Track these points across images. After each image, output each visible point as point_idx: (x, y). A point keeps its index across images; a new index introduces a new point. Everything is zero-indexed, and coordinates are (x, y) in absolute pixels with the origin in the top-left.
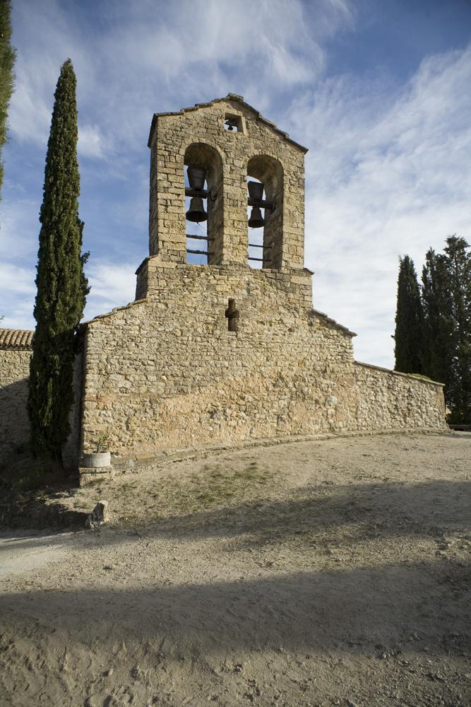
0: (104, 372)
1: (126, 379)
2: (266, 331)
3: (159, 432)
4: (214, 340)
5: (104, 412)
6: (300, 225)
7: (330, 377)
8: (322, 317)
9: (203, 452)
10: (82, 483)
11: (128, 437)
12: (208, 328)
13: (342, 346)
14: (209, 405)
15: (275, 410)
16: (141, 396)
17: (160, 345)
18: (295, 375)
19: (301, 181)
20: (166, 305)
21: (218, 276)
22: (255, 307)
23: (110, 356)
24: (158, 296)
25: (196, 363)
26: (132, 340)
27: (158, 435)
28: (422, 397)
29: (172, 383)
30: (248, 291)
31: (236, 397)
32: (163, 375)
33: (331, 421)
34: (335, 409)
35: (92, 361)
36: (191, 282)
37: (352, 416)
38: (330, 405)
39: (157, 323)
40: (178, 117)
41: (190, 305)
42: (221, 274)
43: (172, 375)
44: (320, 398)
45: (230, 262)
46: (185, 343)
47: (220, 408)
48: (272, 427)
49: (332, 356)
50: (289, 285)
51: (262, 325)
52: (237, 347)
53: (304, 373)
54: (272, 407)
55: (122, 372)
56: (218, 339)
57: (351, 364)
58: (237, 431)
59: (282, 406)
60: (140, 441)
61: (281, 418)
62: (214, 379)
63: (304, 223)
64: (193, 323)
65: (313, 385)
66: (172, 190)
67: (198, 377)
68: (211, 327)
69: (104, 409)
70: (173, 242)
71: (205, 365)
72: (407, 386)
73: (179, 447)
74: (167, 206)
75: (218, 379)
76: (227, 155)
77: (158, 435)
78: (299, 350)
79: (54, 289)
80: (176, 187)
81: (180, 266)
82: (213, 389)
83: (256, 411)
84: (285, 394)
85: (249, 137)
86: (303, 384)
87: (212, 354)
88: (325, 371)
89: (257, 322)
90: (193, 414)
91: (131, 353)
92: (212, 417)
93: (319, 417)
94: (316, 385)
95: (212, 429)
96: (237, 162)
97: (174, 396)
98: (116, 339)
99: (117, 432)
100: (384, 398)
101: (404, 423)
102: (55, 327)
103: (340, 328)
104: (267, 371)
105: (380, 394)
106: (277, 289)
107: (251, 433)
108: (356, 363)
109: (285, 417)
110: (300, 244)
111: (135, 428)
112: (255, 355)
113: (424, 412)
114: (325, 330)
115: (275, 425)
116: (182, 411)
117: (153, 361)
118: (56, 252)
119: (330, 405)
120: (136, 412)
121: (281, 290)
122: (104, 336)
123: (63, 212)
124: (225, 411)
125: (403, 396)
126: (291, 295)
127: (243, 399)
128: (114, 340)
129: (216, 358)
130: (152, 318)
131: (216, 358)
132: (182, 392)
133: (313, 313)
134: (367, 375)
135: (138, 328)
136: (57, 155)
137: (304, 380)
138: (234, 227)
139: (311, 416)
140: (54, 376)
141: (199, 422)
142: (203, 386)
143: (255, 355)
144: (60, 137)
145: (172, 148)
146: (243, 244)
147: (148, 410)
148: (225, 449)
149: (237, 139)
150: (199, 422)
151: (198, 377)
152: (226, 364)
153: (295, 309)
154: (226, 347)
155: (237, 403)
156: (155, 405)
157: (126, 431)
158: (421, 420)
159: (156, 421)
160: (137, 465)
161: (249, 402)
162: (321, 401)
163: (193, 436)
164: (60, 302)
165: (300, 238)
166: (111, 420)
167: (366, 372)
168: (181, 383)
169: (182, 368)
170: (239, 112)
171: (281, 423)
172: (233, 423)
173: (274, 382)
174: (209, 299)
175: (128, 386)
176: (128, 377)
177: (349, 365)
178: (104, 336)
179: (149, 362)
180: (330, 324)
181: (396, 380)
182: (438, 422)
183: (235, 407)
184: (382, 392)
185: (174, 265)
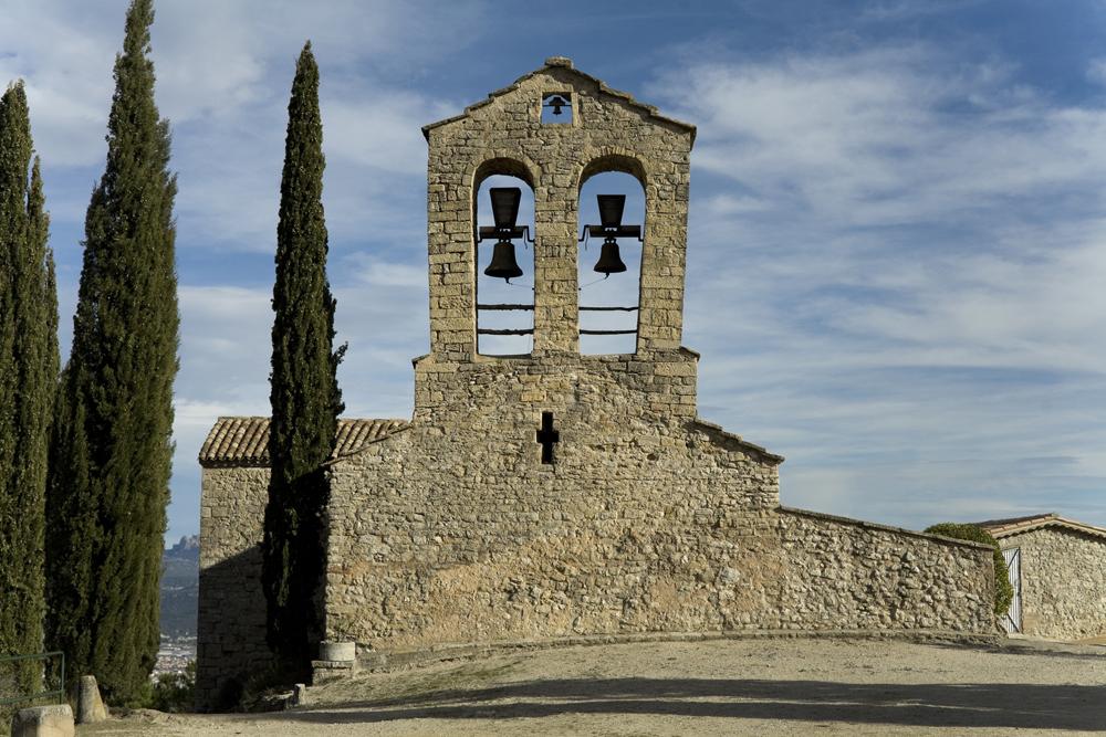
0: (352, 532)
1: (383, 541)
2: (604, 462)
3: (429, 619)
4: (515, 480)
5: (352, 588)
6: (677, 270)
7: (727, 536)
8: (713, 431)
9: (485, 649)
10: (315, 680)
11: (385, 624)
12: (506, 462)
13: (754, 480)
14: (507, 580)
15: (618, 590)
16: (404, 566)
17: (432, 490)
18: (657, 533)
19: (680, 188)
20: (443, 430)
21: (525, 377)
22: (587, 422)
23: (361, 510)
24: (431, 416)
25: (488, 517)
26: (392, 485)
27: (426, 622)
28: (937, 571)
29: (450, 547)
30: (577, 396)
31: (550, 569)
32: (437, 535)
33: (726, 611)
34: (736, 590)
35: (336, 517)
36: (481, 391)
37: (772, 604)
38: (724, 584)
39: (429, 458)
40: (461, 122)
41: (479, 427)
42: (529, 374)
43: (450, 535)
44: (704, 571)
45: (546, 351)
46: (470, 486)
47: (524, 585)
48: (612, 617)
49: (730, 497)
50: (651, 380)
51: (598, 451)
52: (554, 490)
53: (675, 529)
54: (613, 585)
55: (377, 532)
56: (523, 478)
57: (770, 512)
58: (551, 622)
59: (631, 584)
60: (402, 630)
61: (630, 604)
62: (514, 541)
63: (683, 265)
64: (483, 455)
65: (692, 549)
66: (450, 248)
67: (489, 538)
68: (512, 460)
69: (352, 584)
70: (452, 331)
71: (501, 520)
72: (900, 550)
73: (458, 641)
74: (443, 274)
75: (520, 540)
76: (543, 170)
77: (426, 622)
78: (665, 489)
79: (290, 414)
80: (457, 241)
81: (464, 367)
82: (512, 556)
83: (584, 591)
84: (638, 565)
85: (584, 128)
86: (672, 547)
87: (513, 501)
88: (717, 525)
89: (591, 446)
90: (480, 593)
91: (390, 504)
92: (510, 599)
93: (701, 604)
94: (699, 547)
95: (509, 616)
96: (561, 180)
97: (453, 566)
98: (370, 484)
99: (370, 617)
100: (844, 572)
101: (889, 620)
102: (291, 468)
103: (748, 449)
104: (603, 526)
105: (836, 565)
106: (629, 388)
107: (574, 625)
108: (779, 510)
109: (636, 602)
110: (675, 304)
111: (394, 611)
112: (585, 501)
113: (939, 601)
114: (721, 454)
115: (618, 614)
116: (463, 588)
117: (423, 514)
118: (291, 359)
119: (724, 584)
120: (396, 589)
121: (637, 389)
122: (352, 482)
123: (300, 299)
124: (531, 590)
125: (889, 569)
126: (655, 397)
127: (562, 571)
128: (366, 486)
129: (519, 507)
130: (420, 451)
131: (519, 507)
132: (466, 561)
133: (694, 426)
134: (807, 531)
135: (400, 467)
136: (290, 210)
137: (674, 541)
138: (553, 292)
139: (686, 601)
140: (291, 537)
141: (490, 605)
142: (496, 552)
143: (585, 501)
144: (295, 181)
145: (451, 178)
146: (568, 319)
147: (413, 587)
148: (520, 646)
149: (561, 136)
150: (490, 605)
151: (489, 538)
152: (536, 516)
153: (663, 420)
154: (536, 490)
155: (551, 578)
156: (423, 580)
157: (382, 615)
158: (933, 615)
159: (424, 602)
160: (389, 662)
161: (571, 576)
162: (705, 576)
163: (479, 625)
164: (298, 434)
165: (674, 295)
166: (362, 600)
167: (804, 526)
168: (463, 547)
169: (465, 524)
170: (567, 85)
171: (629, 611)
172: (545, 609)
173: (619, 545)
174: (510, 416)
175: (385, 552)
176: (385, 539)
177: (767, 513)
178: (352, 482)
179: (416, 516)
180: (731, 443)
181: (875, 539)
182: (975, 619)
183: (548, 584)
184: (839, 561)
185: (453, 367)
